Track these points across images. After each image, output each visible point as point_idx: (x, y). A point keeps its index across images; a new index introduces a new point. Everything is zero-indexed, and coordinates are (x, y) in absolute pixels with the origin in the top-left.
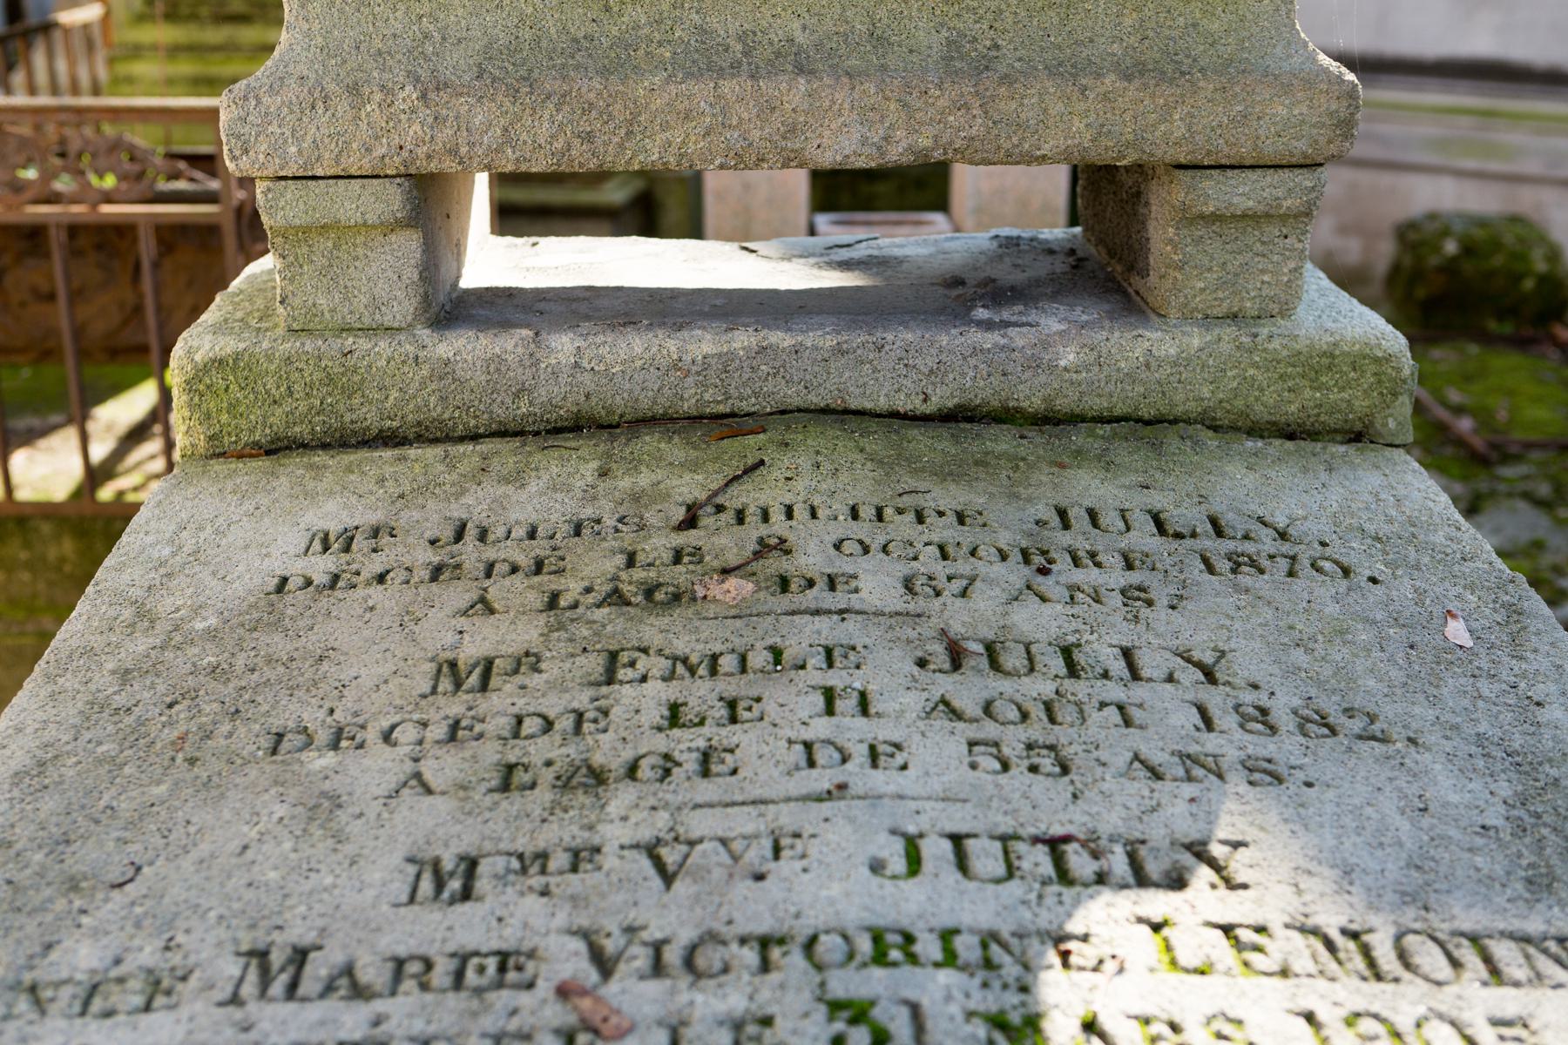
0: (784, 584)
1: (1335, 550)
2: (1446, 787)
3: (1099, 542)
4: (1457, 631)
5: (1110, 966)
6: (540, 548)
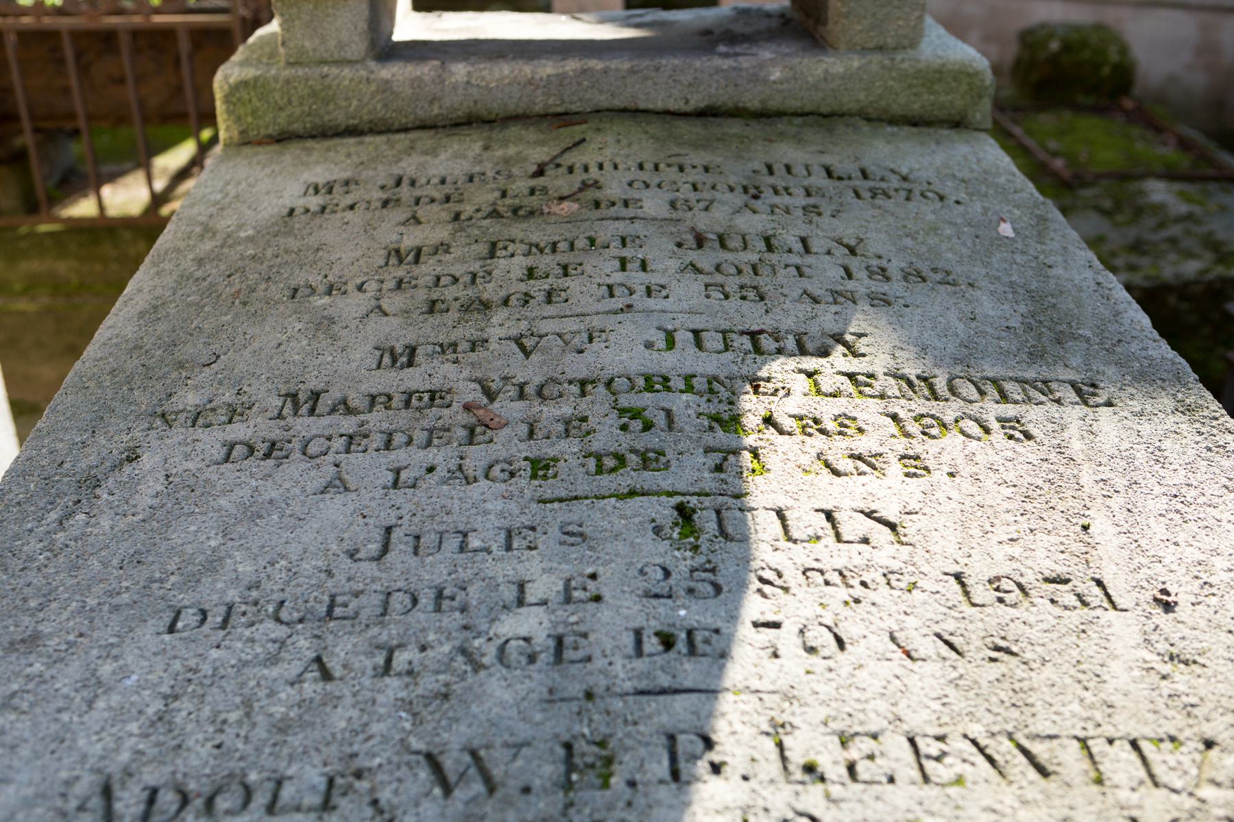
0: (597, 204)
1: (937, 186)
2: (987, 306)
3: (791, 181)
4: (1006, 229)
5: (781, 393)
6: (448, 189)
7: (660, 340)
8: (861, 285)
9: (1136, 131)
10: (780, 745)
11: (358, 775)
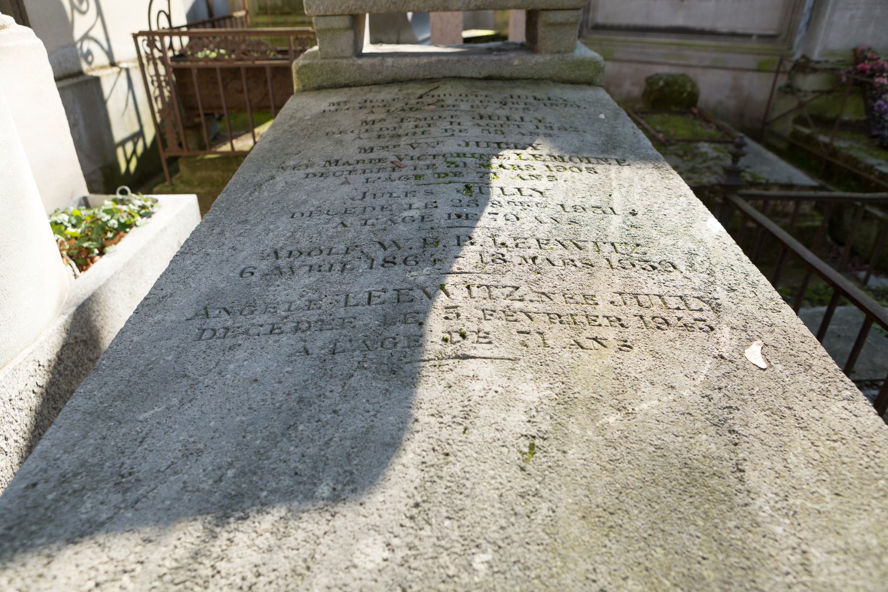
0: (443, 106)
1: (578, 103)
2: (589, 138)
3: (519, 101)
4: (602, 116)
6: (384, 103)
7: (463, 144)
8: (542, 130)
9: (697, 122)
10: (494, 240)
11: (357, 246)
